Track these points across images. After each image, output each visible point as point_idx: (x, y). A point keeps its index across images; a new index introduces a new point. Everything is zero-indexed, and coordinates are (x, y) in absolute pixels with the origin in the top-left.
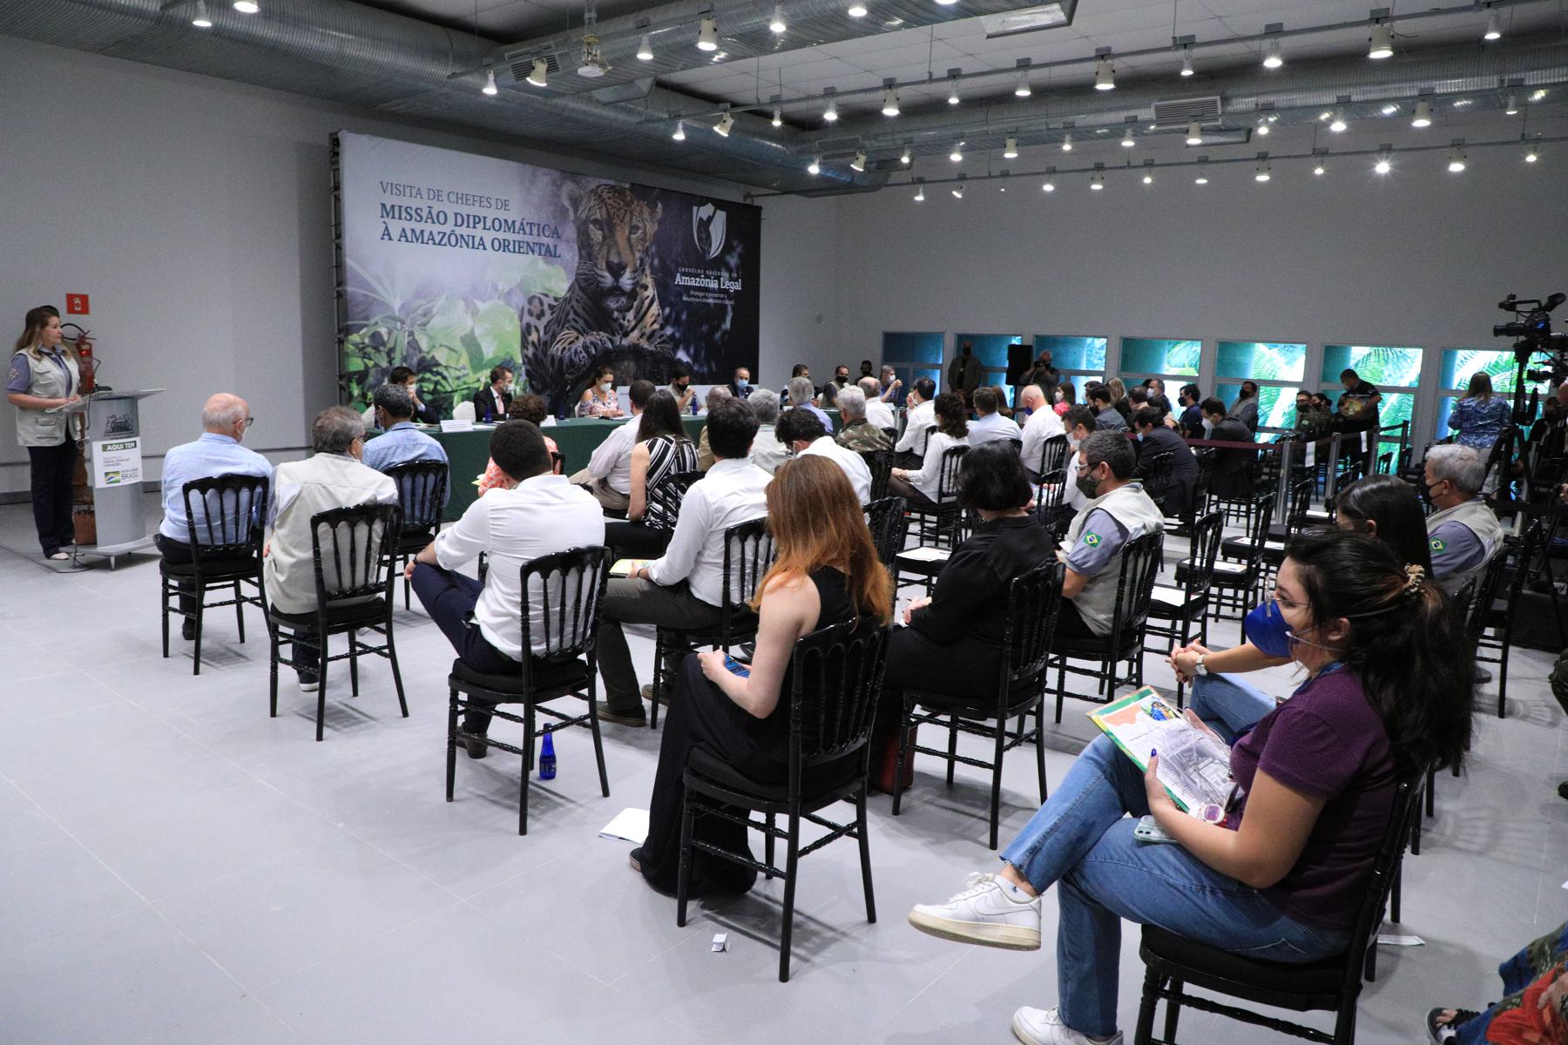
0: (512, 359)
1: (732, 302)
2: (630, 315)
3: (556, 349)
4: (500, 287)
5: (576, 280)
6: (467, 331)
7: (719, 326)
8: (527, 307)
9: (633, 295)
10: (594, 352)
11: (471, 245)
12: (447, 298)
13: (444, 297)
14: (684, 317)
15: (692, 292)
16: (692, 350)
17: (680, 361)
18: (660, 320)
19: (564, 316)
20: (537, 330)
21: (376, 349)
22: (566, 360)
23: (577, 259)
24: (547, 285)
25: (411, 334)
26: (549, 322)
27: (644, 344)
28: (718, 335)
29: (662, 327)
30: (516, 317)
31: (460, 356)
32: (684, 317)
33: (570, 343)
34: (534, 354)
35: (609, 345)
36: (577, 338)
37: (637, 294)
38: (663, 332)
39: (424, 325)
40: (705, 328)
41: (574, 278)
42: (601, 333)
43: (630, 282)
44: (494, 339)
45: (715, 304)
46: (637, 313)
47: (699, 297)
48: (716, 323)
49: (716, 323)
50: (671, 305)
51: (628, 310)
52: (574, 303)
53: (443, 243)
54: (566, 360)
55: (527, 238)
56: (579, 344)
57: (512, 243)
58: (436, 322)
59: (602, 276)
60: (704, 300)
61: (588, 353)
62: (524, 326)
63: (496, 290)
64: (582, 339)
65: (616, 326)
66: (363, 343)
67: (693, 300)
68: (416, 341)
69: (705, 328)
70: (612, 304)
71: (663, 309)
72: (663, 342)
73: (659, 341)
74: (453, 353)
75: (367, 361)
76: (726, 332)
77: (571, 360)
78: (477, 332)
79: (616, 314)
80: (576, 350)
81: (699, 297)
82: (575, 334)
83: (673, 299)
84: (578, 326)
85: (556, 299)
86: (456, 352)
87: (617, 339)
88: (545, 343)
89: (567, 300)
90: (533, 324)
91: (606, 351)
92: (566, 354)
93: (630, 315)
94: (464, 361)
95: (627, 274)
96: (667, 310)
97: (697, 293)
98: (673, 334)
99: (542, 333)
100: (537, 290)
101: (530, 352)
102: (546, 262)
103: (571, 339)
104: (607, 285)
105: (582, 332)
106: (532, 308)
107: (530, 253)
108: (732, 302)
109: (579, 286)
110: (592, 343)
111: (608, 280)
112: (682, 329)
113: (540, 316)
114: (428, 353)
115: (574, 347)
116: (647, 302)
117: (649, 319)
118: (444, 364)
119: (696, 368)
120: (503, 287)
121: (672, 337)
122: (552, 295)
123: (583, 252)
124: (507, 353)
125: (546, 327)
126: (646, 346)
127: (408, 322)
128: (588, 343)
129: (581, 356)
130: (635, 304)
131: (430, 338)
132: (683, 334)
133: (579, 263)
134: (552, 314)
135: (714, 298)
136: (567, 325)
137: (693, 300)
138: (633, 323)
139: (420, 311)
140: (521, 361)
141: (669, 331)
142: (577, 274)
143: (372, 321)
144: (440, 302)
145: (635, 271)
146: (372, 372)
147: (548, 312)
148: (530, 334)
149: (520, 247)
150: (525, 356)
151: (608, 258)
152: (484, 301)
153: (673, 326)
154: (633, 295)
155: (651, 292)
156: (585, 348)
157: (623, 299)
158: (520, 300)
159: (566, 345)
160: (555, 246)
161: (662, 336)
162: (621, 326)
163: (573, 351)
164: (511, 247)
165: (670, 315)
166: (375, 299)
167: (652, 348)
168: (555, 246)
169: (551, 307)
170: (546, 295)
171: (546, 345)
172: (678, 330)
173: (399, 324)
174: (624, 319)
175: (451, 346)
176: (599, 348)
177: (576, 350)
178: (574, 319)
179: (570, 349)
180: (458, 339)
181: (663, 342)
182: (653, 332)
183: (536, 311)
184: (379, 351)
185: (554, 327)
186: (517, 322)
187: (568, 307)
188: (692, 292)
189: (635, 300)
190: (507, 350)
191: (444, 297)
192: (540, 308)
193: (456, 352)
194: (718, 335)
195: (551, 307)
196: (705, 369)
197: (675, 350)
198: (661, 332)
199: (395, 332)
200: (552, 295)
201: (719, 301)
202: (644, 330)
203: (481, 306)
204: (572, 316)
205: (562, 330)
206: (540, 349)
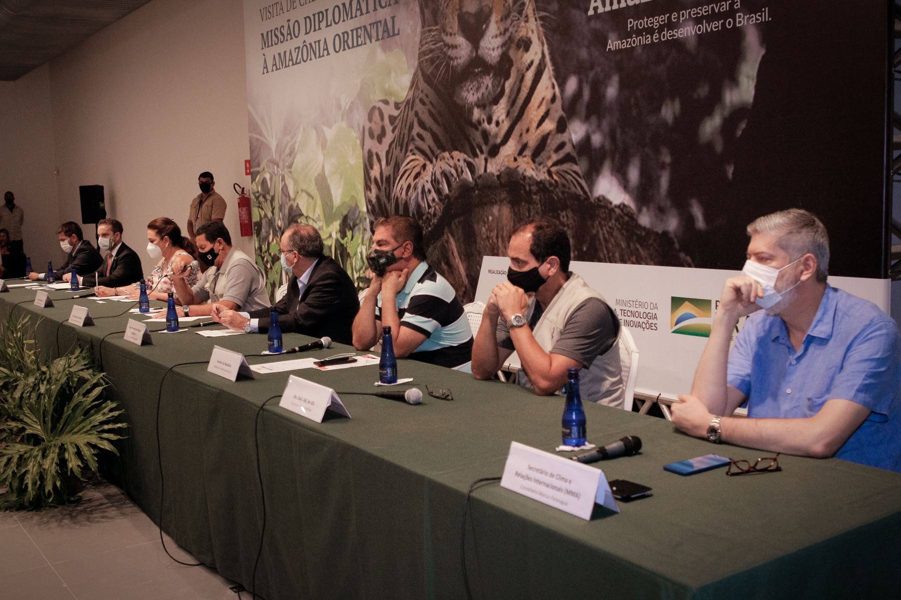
0: (357, 206)
1: (765, 16)
2: (500, 111)
3: (399, 189)
4: (343, 104)
5: (420, 63)
6: (319, 171)
7: (716, 98)
8: (368, 125)
9: (503, 67)
10: (446, 190)
11: (317, 55)
12: (304, 130)
13: (301, 129)
14: (612, 91)
15: (631, 23)
16: (634, 174)
17: (603, 203)
18: (558, 111)
19: (406, 132)
20: (379, 161)
21: (264, 197)
22: (412, 207)
23: (419, 29)
24: (387, 86)
25: (283, 179)
26: (390, 146)
27: (528, 169)
28: (711, 126)
29: (562, 127)
30: (358, 142)
31: (316, 203)
32: (612, 91)
33: (416, 177)
34: (378, 198)
35: (468, 176)
36: (424, 167)
37: (511, 63)
38: (564, 137)
39: (290, 166)
40: (669, 112)
41: (416, 63)
42: (456, 154)
43: (499, 41)
44: (341, 177)
45: (701, 38)
46: (513, 103)
47: (650, 31)
48: (703, 91)
49: (703, 91)
50: (581, 70)
51: (496, 101)
52: (418, 106)
53: (298, 61)
54: (412, 207)
55: (365, 20)
56: (427, 177)
57: (350, 33)
58: (299, 161)
59: (454, 47)
60: (667, 35)
61: (439, 192)
62: (367, 155)
63: (340, 107)
64: (430, 167)
65: (478, 137)
66: (258, 192)
67: (636, 41)
68: (287, 188)
69: (669, 112)
70: (470, 95)
71: (562, 84)
72: (568, 159)
73: (555, 157)
74: (311, 200)
75: (260, 210)
76: (739, 112)
77: (418, 206)
78: (327, 173)
79: (477, 114)
80: (423, 187)
81: (650, 31)
82: (421, 160)
83: (584, 54)
84: (425, 147)
85: (397, 105)
86: (313, 198)
87: (479, 162)
88: (388, 178)
89: (410, 103)
90: (374, 151)
91: (465, 188)
92: (413, 195)
93: (500, 111)
94: (319, 211)
95: (493, 28)
96: (572, 84)
97: (645, 22)
98: (587, 139)
99: (384, 163)
100: (376, 97)
101: (373, 195)
102: (385, 49)
103: (417, 170)
104: (461, 61)
105: (430, 157)
106: (373, 126)
107: (368, 41)
108: (765, 16)
109: (424, 74)
110: (444, 174)
111: (462, 50)
112: (605, 124)
113: (380, 139)
114: (294, 200)
115: (421, 182)
116: (530, 75)
117: (534, 113)
118: (305, 214)
119: (645, 220)
120: (345, 102)
121: (584, 146)
122: (392, 100)
123: (427, 12)
124: (353, 196)
125: (388, 153)
126: (530, 172)
127: (281, 165)
128: (439, 176)
129: (430, 198)
130: (508, 85)
131: (296, 182)
132: (612, 136)
133: (423, 33)
134: (393, 131)
135: (698, 21)
136: (411, 147)
137: (636, 41)
138: (505, 126)
139: (287, 151)
140: (365, 209)
141: (577, 131)
142: (419, 58)
143: (262, 167)
144: (299, 138)
145: (504, 18)
146: (264, 222)
147: (389, 128)
148: (372, 168)
149: (358, 37)
150: (369, 201)
151: (461, 8)
152: (330, 127)
153: (587, 119)
154: (503, 67)
155: (536, 52)
156: (435, 182)
157: (488, 81)
158: (360, 117)
159: (410, 180)
160: (393, 18)
161: (562, 146)
162: (485, 135)
163: (420, 190)
164: (350, 42)
165: (578, 94)
166: (262, 142)
167: (542, 176)
168: (393, 18)
169: (392, 119)
170: (386, 102)
171: (388, 182)
172: (599, 126)
173: (275, 167)
174: (490, 121)
175: (309, 191)
176: (454, 185)
177: (423, 187)
178: (419, 135)
179: (415, 188)
180: (313, 179)
181: (568, 159)
182: (543, 142)
183: (377, 132)
184: (266, 200)
185: (396, 152)
186: (359, 152)
187: (411, 114)
188: (631, 23)
189: (507, 77)
190: (353, 194)
191: (301, 129)
192: (380, 124)
193: (313, 198)
194: (711, 126)
195: (392, 119)
196: (672, 224)
197: (592, 174)
198: (560, 138)
199: (274, 178)
200: (392, 100)
201: (716, 26)
202: (526, 138)
203: (330, 133)
204: (417, 129)
205: (405, 157)
206: (383, 188)
